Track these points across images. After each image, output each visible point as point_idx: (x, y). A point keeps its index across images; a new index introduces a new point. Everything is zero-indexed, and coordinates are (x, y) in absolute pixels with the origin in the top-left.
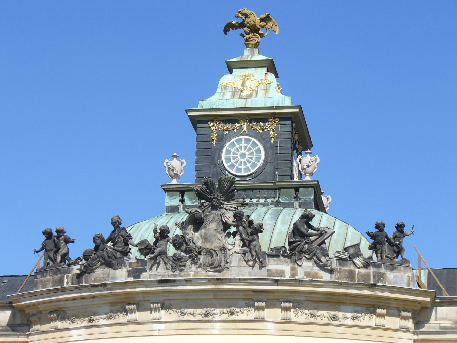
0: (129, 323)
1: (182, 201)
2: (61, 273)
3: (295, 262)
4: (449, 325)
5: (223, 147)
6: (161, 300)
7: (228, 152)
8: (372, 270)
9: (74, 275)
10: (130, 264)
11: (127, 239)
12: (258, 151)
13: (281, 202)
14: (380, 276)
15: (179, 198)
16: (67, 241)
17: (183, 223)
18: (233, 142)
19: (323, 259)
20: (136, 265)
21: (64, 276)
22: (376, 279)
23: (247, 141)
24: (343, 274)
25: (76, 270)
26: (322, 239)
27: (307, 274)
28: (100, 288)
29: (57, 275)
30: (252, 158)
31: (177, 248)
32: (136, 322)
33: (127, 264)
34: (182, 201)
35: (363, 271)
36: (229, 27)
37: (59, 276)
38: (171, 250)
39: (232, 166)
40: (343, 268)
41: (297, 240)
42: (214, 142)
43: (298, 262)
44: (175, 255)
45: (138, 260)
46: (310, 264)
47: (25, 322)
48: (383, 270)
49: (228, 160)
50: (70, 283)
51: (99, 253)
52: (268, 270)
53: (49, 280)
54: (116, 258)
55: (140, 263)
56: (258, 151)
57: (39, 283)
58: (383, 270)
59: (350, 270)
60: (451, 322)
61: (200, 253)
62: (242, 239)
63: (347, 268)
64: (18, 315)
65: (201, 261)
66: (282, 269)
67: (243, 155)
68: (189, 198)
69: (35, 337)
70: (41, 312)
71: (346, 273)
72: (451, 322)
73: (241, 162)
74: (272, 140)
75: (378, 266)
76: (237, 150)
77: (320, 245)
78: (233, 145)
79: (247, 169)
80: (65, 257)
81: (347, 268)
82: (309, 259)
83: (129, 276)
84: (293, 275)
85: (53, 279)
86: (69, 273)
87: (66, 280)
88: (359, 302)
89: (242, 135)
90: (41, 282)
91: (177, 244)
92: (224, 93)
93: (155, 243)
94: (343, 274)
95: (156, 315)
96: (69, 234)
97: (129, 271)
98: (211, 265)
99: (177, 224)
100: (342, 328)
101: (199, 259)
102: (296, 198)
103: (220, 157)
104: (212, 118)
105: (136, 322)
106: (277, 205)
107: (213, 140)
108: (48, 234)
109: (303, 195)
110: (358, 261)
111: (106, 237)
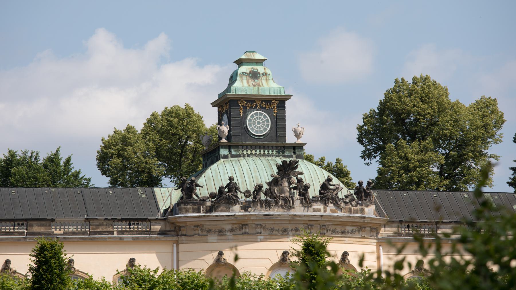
0: (244, 234)
1: (230, 152)
2: (198, 205)
3: (325, 204)
4: (392, 234)
5: (247, 117)
6: (261, 224)
8: (359, 207)
9: (207, 206)
10: (242, 203)
11: (237, 189)
13: (286, 154)
14: (362, 211)
15: (228, 150)
17: (270, 183)
18: (253, 115)
19: (339, 203)
20: (245, 204)
21: (201, 207)
22: (361, 212)
23: (261, 114)
24: (347, 210)
25: (209, 204)
26: (337, 191)
27: (332, 211)
28: (231, 217)
29: (195, 205)
30: (264, 125)
31: (266, 195)
32: (247, 233)
33: (240, 203)
34: (230, 152)
35: (354, 208)
37: (197, 206)
38: (263, 197)
39: (253, 129)
40: (347, 207)
41: (325, 192)
42: (242, 114)
43: (327, 205)
44: (266, 200)
45: (246, 201)
46: (332, 205)
47: (173, 229)
48: (363, 207)
49: (250, 125)
50: (205, 211)
51: (224, 196)
52: (313, 209)
53: (190, 208)
54: (233, 199)
55: (247, 203)
56: (267, 120)
57: (183, 209)
58: (363, 207)
59: (350, 208)
60: (392, 233)
61: (279, 199)
62: (299, 193)
63: (348, 207)
64: (168, 225)
65: (280, 203)
66: (319, 208)
68: (234, 150)
69: (184, 238)
70: (187, 225)
71: (348, 209)
72: (392, 233)
73: (256, 126)
74: (275, 114)
75: (361, 205)
76: (255, 119)
77: (336, 195)
79: (261, 132)
81: (348, 207)
82: (331, 203)
83: (241, 210)
84: (325, 211)
85: (193, 207)
86: (204, 205)
87: (202, 209)
88: (355, 225)
89: (257, 110)
90: (185, 208)
91: (266, 194)
92: (242, 80)
93: (254, 192)
94: (347, 210)
95: (258, 230)
97: (241, 207)
98: (286, 206)
99: (266, 182)
100: (347, 238)
101: (279, 202)
102: (294, 153)
103: (245, 123)
104: (240, 99)
105: (247, 233)
107: (241, 113)
109: (298, 151)
110: (354, 203)
111: (225, 186)
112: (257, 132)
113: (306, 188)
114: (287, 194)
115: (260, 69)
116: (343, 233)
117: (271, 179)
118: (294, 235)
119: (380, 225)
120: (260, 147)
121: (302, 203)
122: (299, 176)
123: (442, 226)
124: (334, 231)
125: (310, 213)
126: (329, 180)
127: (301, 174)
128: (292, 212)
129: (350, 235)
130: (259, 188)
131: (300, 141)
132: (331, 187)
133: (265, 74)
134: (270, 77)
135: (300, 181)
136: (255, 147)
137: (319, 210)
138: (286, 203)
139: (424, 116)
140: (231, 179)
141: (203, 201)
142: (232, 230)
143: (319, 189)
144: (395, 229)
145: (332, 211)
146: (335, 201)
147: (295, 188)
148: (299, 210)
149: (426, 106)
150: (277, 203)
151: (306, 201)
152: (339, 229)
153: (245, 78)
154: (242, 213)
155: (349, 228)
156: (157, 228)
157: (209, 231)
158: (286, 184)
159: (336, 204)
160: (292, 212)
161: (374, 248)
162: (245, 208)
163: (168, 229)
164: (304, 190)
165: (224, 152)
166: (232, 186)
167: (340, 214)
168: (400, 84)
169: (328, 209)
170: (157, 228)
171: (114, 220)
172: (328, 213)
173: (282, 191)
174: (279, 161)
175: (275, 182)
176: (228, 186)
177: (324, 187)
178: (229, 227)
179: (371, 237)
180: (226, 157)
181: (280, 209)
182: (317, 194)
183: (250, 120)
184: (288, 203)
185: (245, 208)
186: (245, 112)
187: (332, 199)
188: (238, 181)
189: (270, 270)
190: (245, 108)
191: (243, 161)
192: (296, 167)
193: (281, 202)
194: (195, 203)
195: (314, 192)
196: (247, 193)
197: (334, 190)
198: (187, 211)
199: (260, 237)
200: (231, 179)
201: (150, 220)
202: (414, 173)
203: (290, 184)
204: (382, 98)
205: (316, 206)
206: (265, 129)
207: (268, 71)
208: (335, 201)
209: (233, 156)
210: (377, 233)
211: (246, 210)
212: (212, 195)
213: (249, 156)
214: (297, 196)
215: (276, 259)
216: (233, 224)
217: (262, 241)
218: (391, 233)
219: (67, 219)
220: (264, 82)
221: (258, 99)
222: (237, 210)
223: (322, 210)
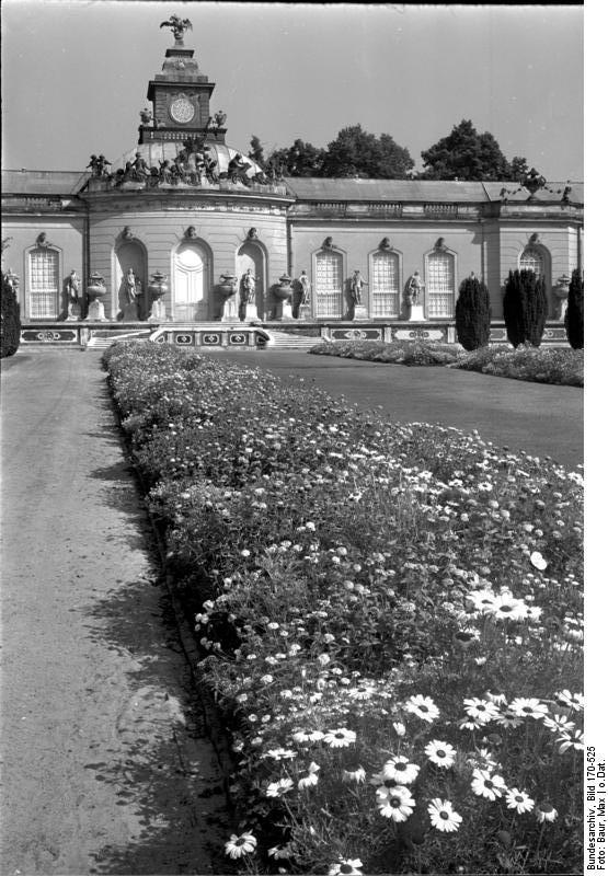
11: (144, 165)
16: (106, 163)
36: (166, 24)
108: (93, 158)
111: (132, 162)
113: (214, 165)
114: (194, 170)
117: (175, 156)
130: (165, 164)
131: (222, 127)
147: (202, 166)
164: (210, 167)
166: (139, 162)
173: (187, 167)
175: (181, 158)
176: (135, 163)
177: (232, 164)
188: (144, 157)
197: (242, 169)
212: (120, 172)
214: (204, 173)
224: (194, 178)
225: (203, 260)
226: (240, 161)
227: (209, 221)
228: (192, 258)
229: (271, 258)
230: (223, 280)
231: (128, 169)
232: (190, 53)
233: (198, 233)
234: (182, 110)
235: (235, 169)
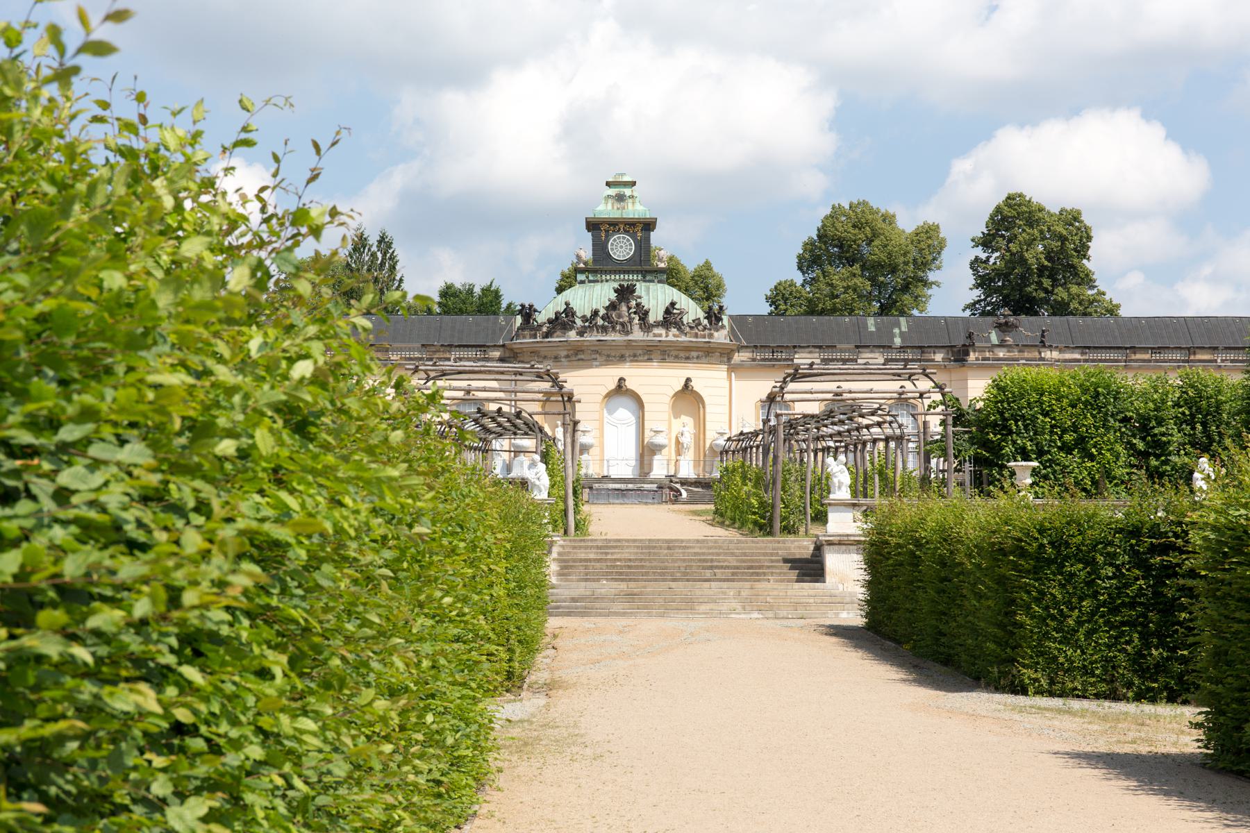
1: (587, 277)
7: (612, 244)
8: (707, 332)
11: (573, 314)
12: (631, 245)
14: (711, 336)
16: (535, 311)
23: (624, 238)
25: (545, 329)
27: (674, 336)
34: (587, 277)
38: (600, 322)
39: (615, 254)
49: (612, 249)
56: (631, 245)
67: (621, 247)
78: (615, 240)
80: (535, 320)
91: (603, 318)
96: (536, 307)
106: (645, 281)
110: (700, 328)
112: (619, 256)
113: (646, 313)
114: (626, 319)
115: (628, 192)
116: (687, 358)
117: (607, 303)
118: (632, 361)
119: (732, 350)
120: (620, 272)
121: (641, 328)
122: (639, 300)
123: (800, 350)
124: (676, 357)
125: (651, 337)
126: (673, 304)
127: (640, 297)
128: (630, 337)
129: (695, 361)
130: (595, 313)
132: (675, 311)
133: (632, 197)
134: (637, 200)
135: (638, 305)
136: (615, 272)
137: (660, 335)
138: (623, 327)
139: (854, 241)
140: (567, 304)
141: (540, 326)
142: (567, 356)
143: (662, 313)
144: (750, 355)
145: (674, 336)
146: (679, 325)
147: (635, 313)
148: (637, 335)
149: (857, 231)
150: (614, 328)
151: (645, 326)
152: (682, 354)
153: (610, 201)
154: (579, 338)
155: (694, 354)
156: (497, 354)
157: (545, 357)
158: (624, 308)
159: (679, 329)
160: (630, 337)
161: (725, 374)
162: (581, 334)
163: (507, 355)
164: (643, 314)
165: (580, 277)
166: (569, 311)
167: (683, 338)
168: (836, 212)
169: (670, 334)
170: (497, 354)
171: (451, 346)
172: (671, 338)
173: (620, 316)
174: (616, 285)
175: (613, 306)
178: (563, 353)
179: (721, 363)
180: (582, 282)
181: (618, 334)
182: (660, 318)
183: (612, 244)
184: (626, 330)
185: (581, 334)
186: (607, 236)
187: (675, 323)
189: (605, 397)
190: (607, 231)
191: (598, 286)
192: (634, 291)
193: (618, 327)
194: (533, 329)
195: (656, 315)
196: (584, 319)
197: (679, 314)
198: (524, 337)
199: (595, 363)
200: (567, 304)
201: (488, 347)
202: (838, 300)
203: (629, 308)
204: (820, 225)
205: (656, 331)
206: (628, 254)
207: (635, 194)
208: (679, 325)
209: (590, 281)
210: (729, 359)
211: (582, 336)
212: (550, 321)
213: (607, 281)
214: (636, 321)
215: (612, 385)
216: (569, 350)
217: (597, 366)
218: (745, 359)
219: (403, 345)
220: (630, 205)
221: (621, 223)
222: (572, 335)
223: (664, 335)
224: (626, 330)
225: (633, 413)
226: (676, 306)
227: (640, 376)
228: (624, 414)
229: (708, 409)
230: (653, 434)
231: (557, 318)
232: (634, 184)
233: (630, 384)
234: (621, 248)
235: (671, 317)
